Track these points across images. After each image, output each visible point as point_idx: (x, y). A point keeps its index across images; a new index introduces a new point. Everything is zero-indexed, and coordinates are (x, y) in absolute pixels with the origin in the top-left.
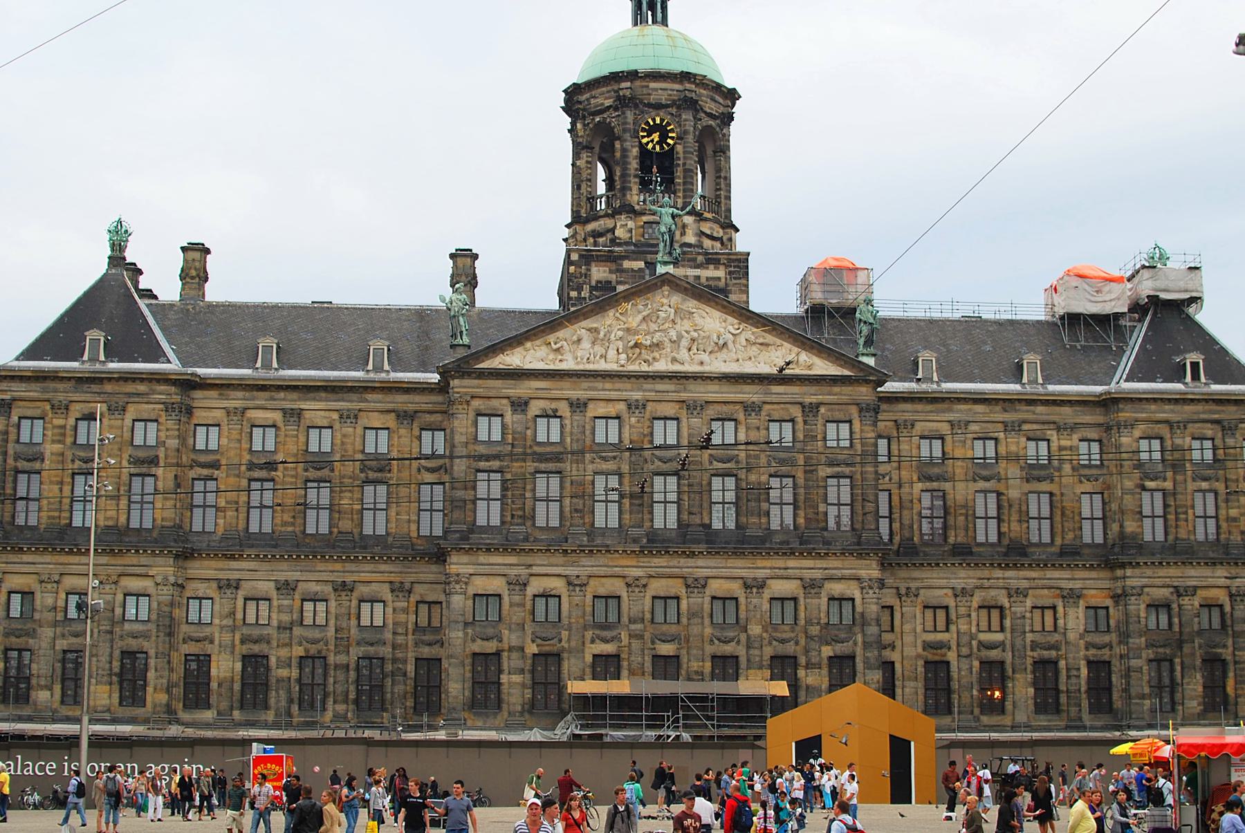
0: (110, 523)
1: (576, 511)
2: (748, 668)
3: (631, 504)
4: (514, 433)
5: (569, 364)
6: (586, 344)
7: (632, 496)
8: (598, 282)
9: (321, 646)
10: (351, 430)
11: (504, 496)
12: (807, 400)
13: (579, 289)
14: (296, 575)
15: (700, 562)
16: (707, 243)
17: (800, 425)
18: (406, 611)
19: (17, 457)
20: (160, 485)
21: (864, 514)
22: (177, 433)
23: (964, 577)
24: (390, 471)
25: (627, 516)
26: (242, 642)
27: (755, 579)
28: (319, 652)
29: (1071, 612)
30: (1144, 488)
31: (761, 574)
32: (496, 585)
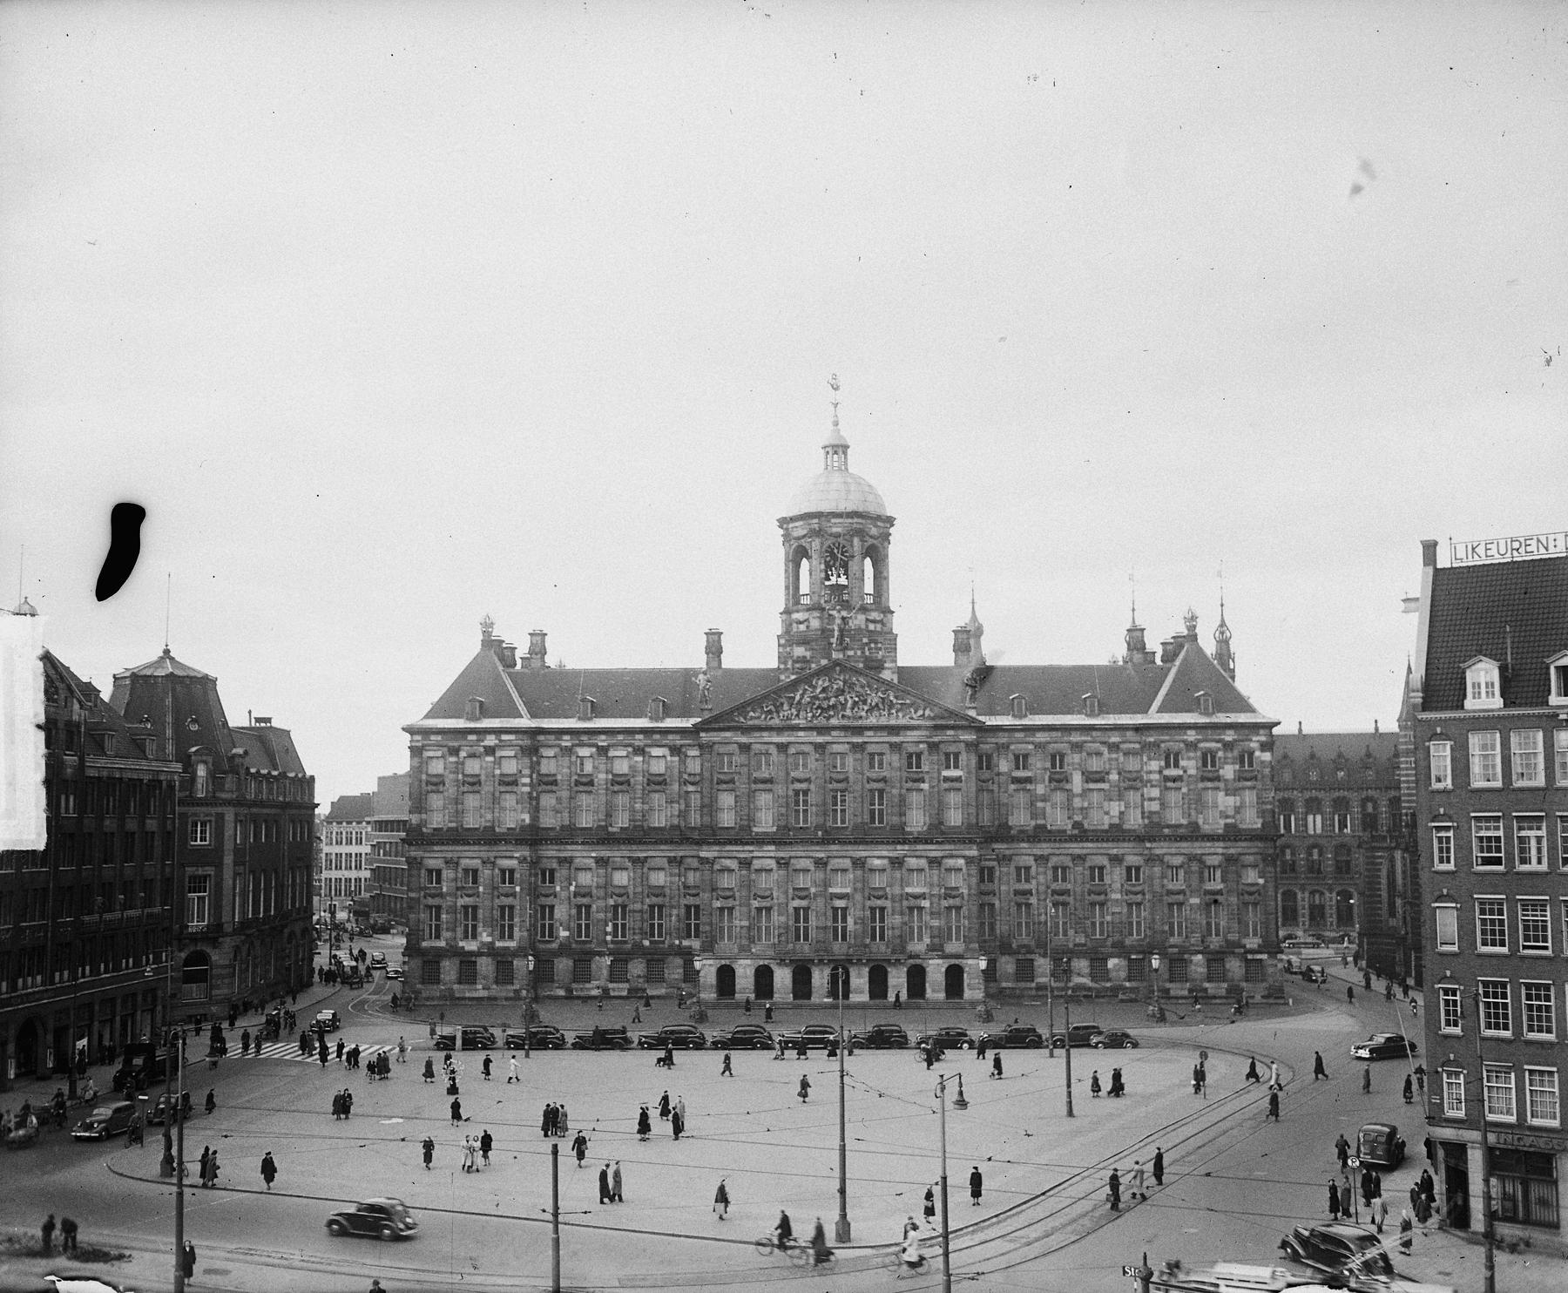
6: (786, 707)
13: (785, 663)
14: (608, 854)
16: (872, 627)
19: (428, 783)
23: (1044, 848)
29: (1117, 871)
30: (1167, 789)
32: (733, 864)
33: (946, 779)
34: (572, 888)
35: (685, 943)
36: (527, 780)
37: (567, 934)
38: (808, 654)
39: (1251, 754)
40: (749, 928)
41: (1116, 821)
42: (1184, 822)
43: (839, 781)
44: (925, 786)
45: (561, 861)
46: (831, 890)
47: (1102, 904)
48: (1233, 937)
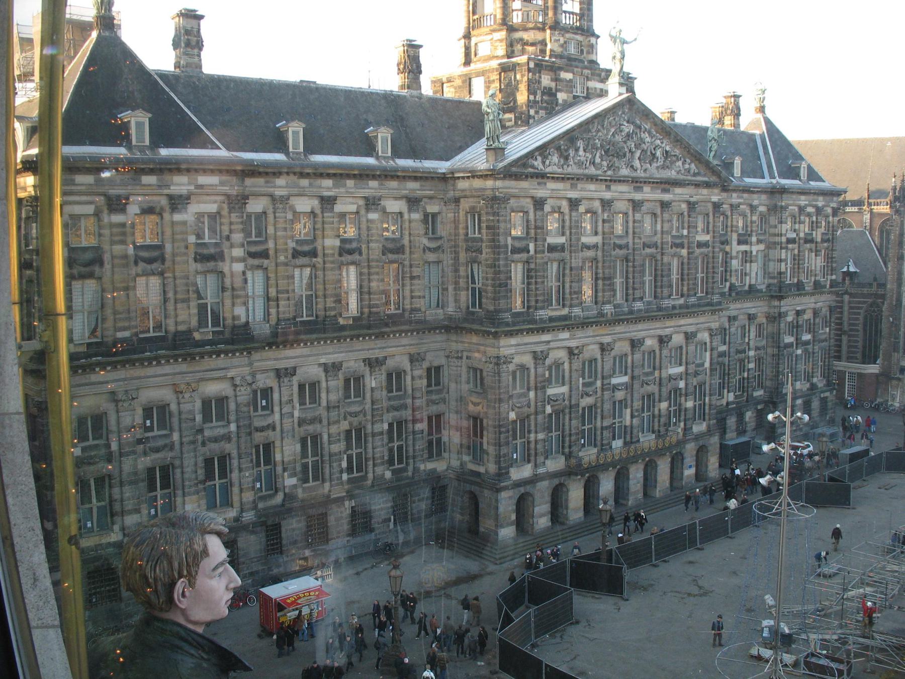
0: (181, 328)
1: (575, 293)
2: (660, 401)
3: (604, 285)
4: (536, 228)
5: (572, 169)
7: (604, 279)
8: (545, 88)
9: (361, 418)
10: (373, 216)
11: (529, 284)
12: (692, 199)
13: (535, 94)
15: (640, 326)
17: (686, 219)
18: (420, 377)
20: (228, 282)
21: (714, 283)
22: (241, 226)
24: (403, 253)
25: (600, 294)
26: (299, 425)
27: (666, 336)
28: (360, 423)
31: (667, 331)
33: (700, 245)
34: (296, 414)
35: (430, 466)
36: (238, 252)
37: (293, 481)
38: (553, 85)
39: (827, 216)
40: (544, 440)
41: (753, 282)
42: (796, 280)
43: (620, 247)
44: (684, 252)
45: (280, 374)
46: (615, 381)
47: (742, 361)
48: (815, 380)
